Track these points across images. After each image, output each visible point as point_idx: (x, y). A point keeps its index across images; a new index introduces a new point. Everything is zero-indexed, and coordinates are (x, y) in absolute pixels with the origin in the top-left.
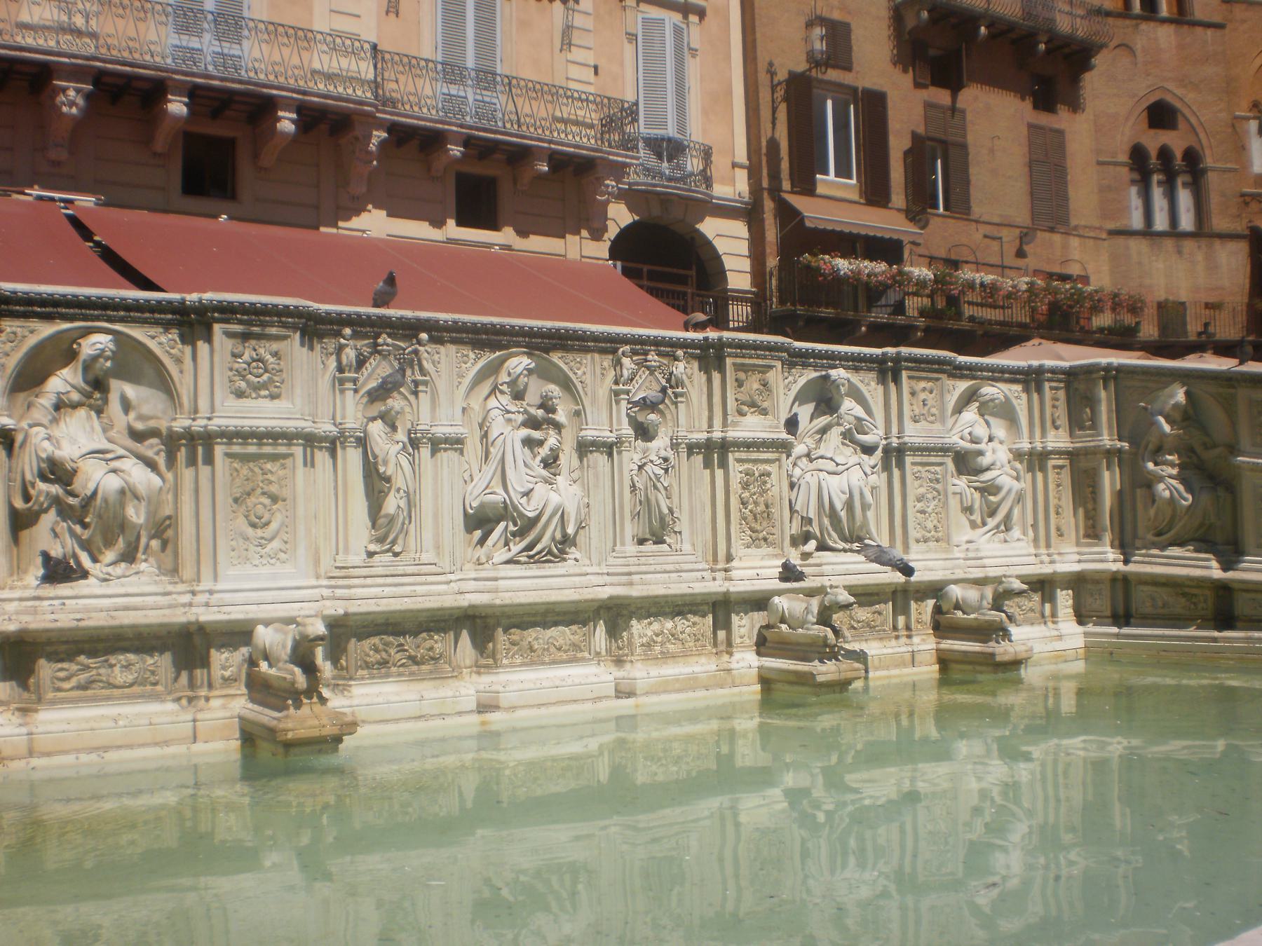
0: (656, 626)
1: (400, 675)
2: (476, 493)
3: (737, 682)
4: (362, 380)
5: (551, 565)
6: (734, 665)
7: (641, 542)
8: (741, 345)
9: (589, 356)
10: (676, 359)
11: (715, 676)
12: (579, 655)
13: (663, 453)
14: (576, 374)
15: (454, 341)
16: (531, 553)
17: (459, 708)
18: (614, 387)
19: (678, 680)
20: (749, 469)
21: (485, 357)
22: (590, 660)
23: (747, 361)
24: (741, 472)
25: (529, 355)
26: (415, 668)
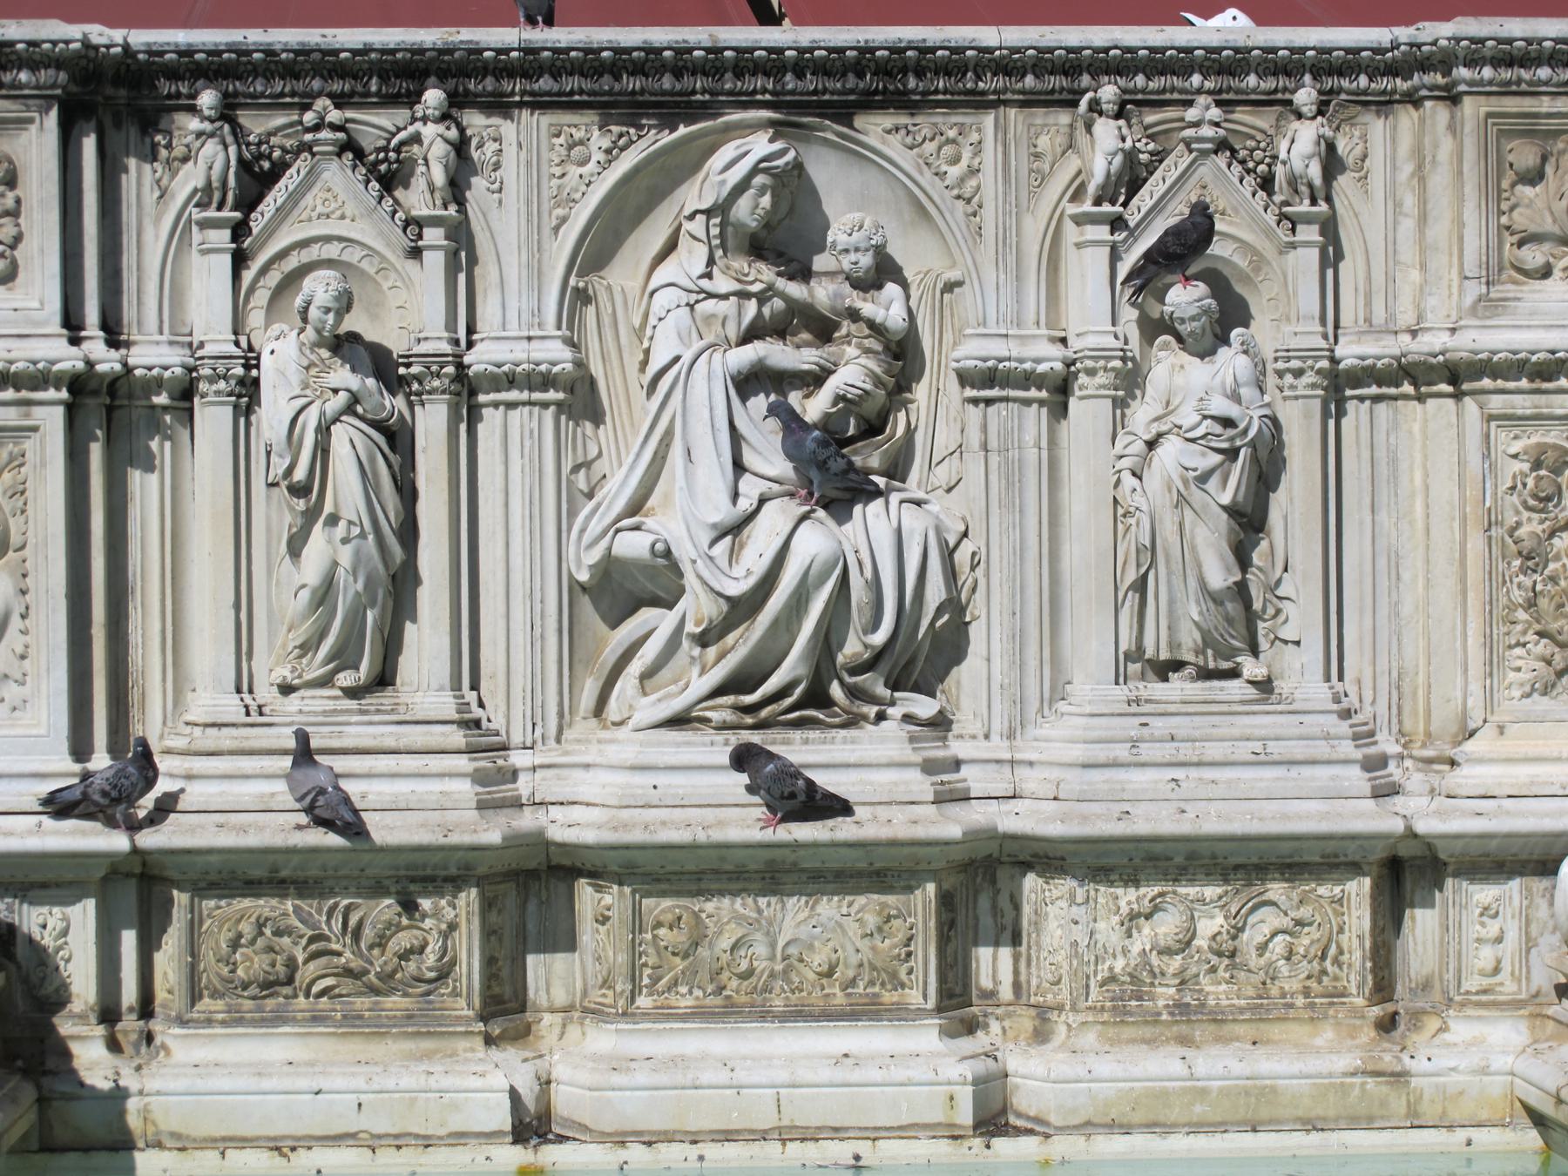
0: (1167, 925)
1: (316, 1019)
2: (595, 527)
3: (1429, 1112)
4: (256, 226)
5: (813, 734)
6: (1418, 1065)
7: (1165, 669)
8: (1510, 57)
9: (988, 120)
10: (1299, 116)
11: (1344, 1089)
12: (889, 997)
13: (1221, 406)
14: (941, 175)
15: (540, 104)
16: (749, 699)
17: (457, 1124)
18: (1073, 209)
19: (1204, 1092)
20: (1542, 448)
21: (642, 144)
22: (920, 1013)
23: (1545, 105)
24: (1515, 456)
25: (779, 129)
26: (362, 1003)
